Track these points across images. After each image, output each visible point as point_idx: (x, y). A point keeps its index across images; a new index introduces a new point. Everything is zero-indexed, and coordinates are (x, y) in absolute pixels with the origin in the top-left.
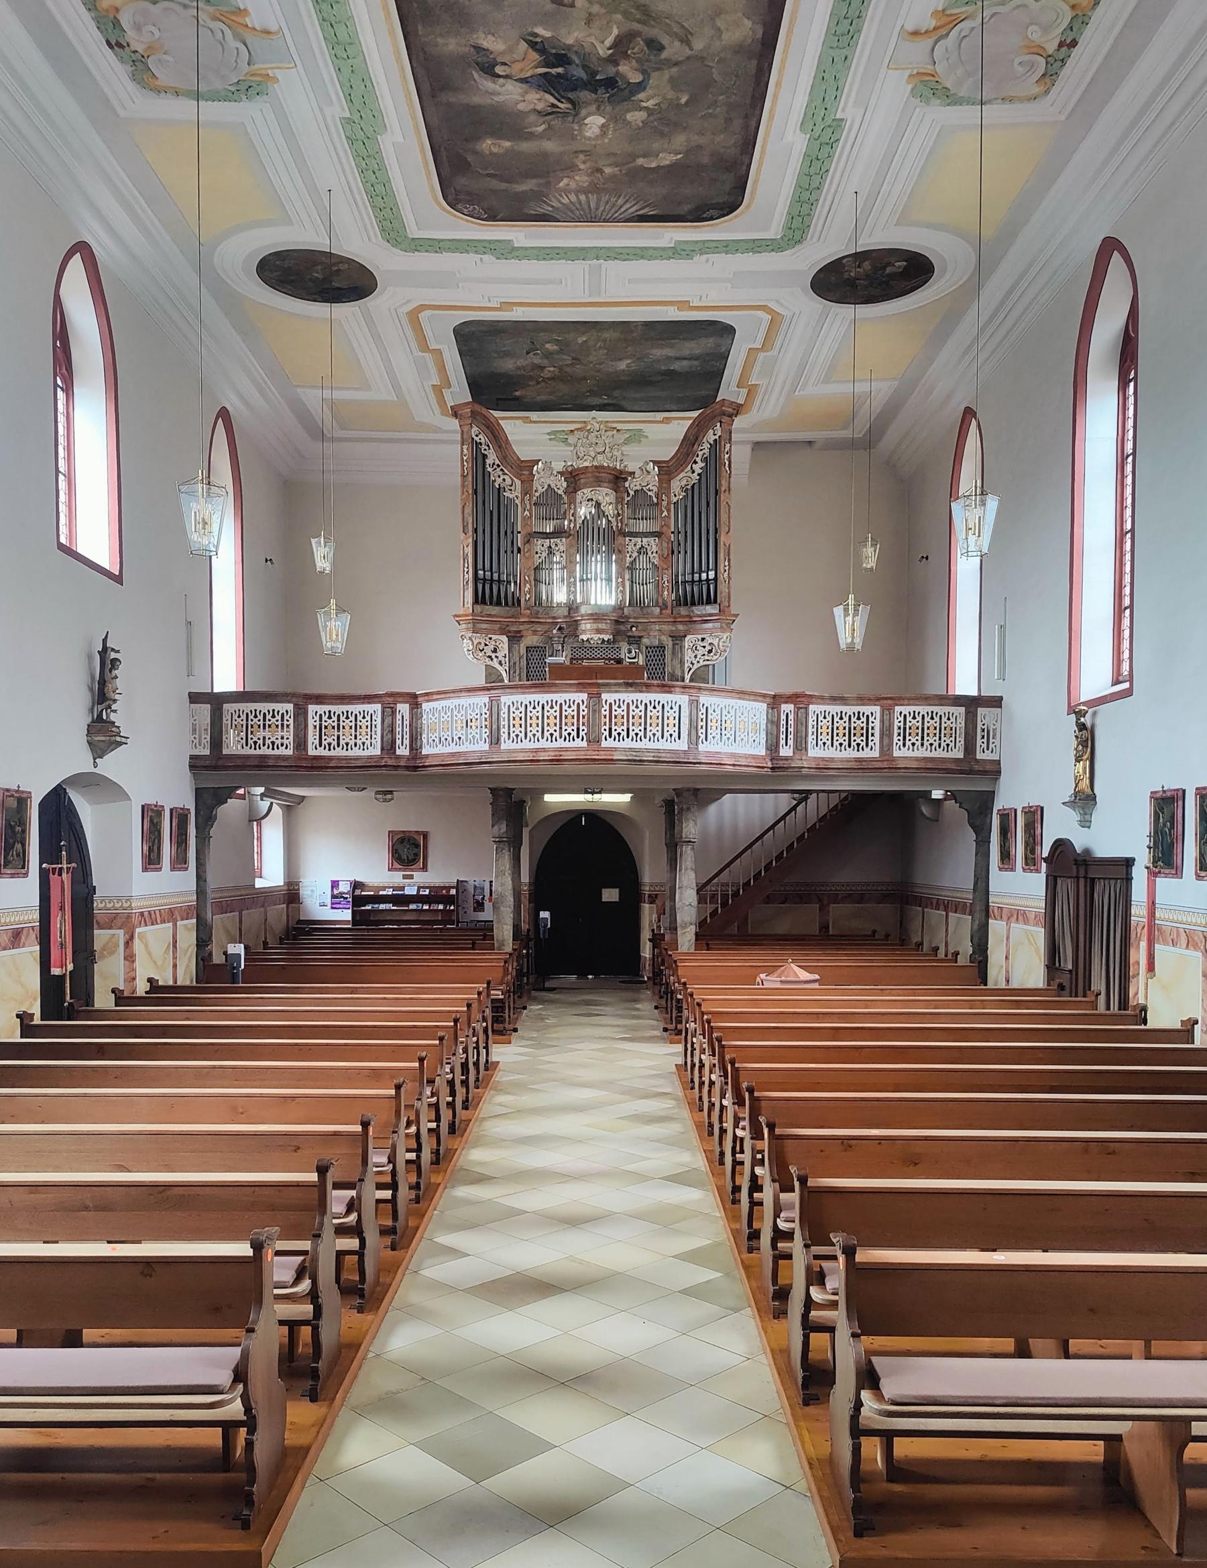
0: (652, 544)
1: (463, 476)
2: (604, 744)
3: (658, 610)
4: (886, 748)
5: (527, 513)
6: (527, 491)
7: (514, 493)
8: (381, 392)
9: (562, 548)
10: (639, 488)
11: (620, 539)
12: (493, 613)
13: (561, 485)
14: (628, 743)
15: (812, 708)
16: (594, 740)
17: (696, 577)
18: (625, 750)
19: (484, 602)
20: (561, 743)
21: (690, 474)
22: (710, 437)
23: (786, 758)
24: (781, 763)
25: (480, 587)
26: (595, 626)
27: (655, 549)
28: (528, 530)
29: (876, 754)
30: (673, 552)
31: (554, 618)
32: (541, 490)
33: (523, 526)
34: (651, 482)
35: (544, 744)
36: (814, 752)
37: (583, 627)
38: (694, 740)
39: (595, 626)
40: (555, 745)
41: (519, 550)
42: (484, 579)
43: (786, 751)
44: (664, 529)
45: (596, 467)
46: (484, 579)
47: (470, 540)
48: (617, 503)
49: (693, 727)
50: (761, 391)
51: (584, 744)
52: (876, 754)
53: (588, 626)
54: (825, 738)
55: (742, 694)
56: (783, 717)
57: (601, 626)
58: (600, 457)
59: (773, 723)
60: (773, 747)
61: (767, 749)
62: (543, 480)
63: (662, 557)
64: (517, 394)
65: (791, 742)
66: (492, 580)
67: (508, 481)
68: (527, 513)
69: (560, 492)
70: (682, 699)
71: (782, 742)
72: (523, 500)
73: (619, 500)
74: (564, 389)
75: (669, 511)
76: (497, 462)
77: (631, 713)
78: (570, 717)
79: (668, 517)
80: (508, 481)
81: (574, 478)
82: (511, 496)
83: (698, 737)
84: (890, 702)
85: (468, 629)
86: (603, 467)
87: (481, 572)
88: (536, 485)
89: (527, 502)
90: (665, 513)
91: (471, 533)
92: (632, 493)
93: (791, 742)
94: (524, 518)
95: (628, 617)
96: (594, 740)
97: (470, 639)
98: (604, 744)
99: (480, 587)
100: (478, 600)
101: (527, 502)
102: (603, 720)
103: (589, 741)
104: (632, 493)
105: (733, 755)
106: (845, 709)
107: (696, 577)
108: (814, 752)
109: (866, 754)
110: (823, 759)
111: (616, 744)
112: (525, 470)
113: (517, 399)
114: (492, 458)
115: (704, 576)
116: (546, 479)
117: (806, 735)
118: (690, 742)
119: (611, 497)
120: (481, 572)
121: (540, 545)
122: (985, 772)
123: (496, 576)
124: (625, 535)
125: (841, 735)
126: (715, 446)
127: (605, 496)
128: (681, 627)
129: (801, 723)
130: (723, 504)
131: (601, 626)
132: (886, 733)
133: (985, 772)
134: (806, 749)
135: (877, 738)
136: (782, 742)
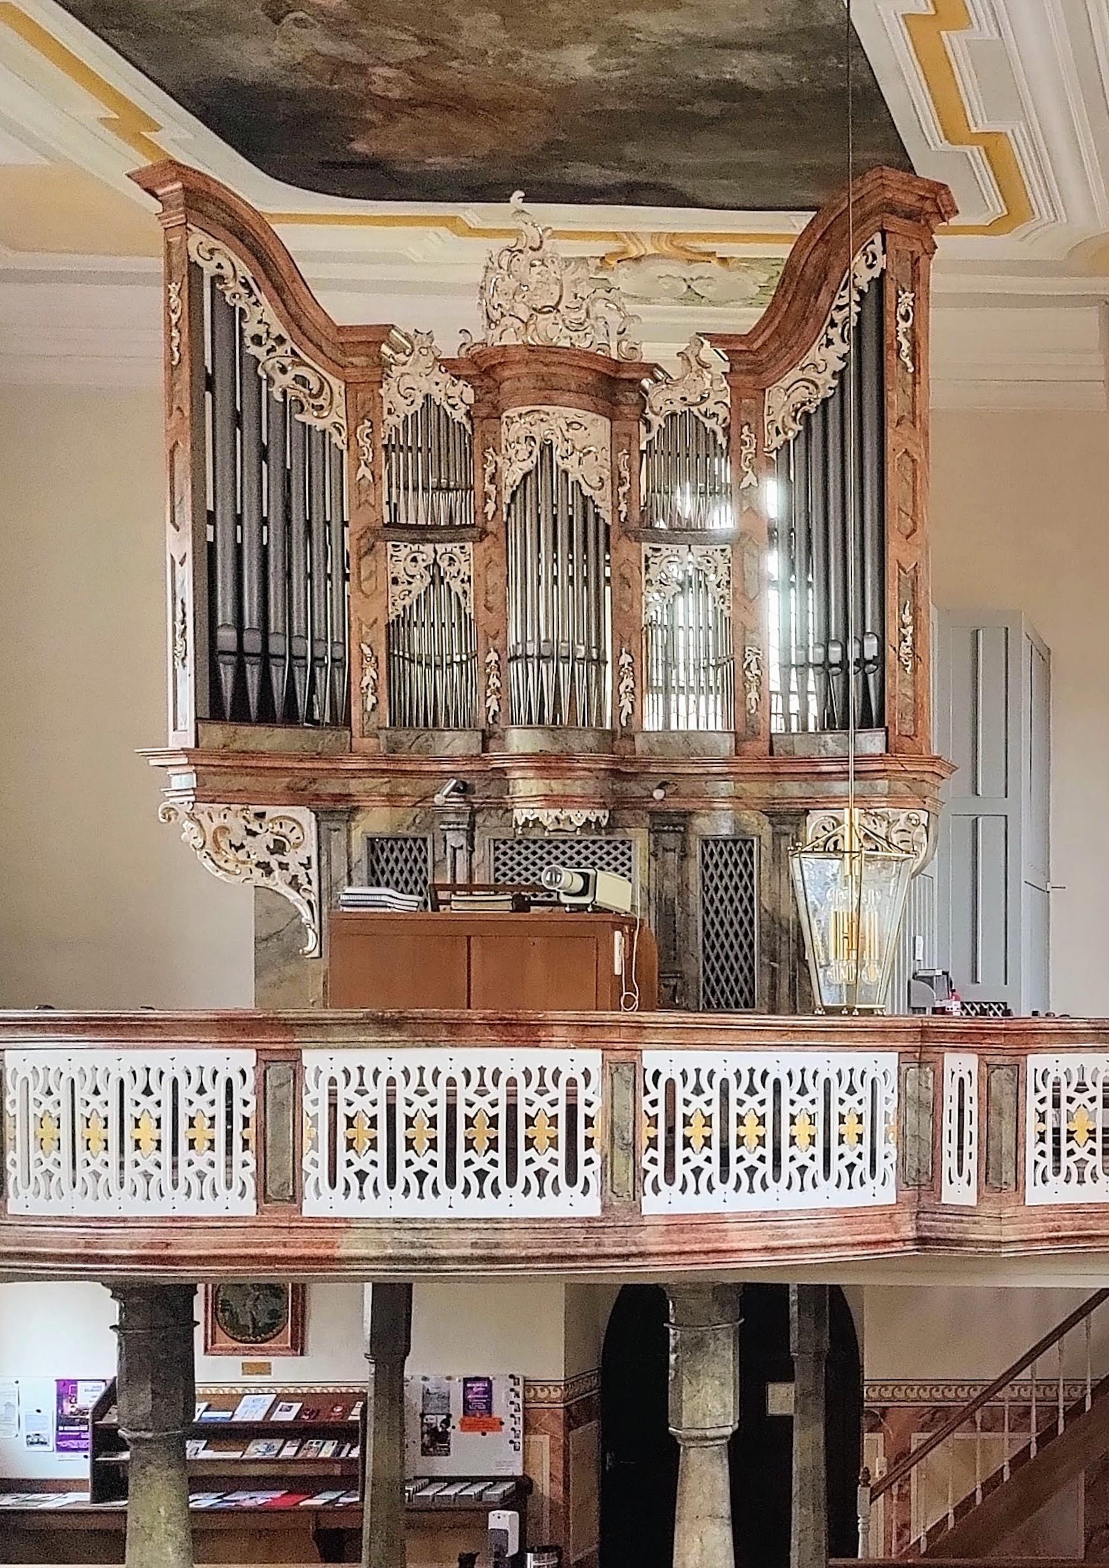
5: (364, 471)
6: (365, 410)
11: (625, 549)
12: (266, 746)
25: (227, 675)
32: (404, 409)
48: (615, 448)
62: (412, 384)
68: (364, 471)
69: (459, 415)
73: (620, 441)
82: (319, 425)
87: (227, 638)
89: (365, 443)
99: (227, 675)
104: (657, 421)
112: (366, 352)
114: (263, 316)
121: (405, 561)
123: (277, 645)
128: (794, 789)
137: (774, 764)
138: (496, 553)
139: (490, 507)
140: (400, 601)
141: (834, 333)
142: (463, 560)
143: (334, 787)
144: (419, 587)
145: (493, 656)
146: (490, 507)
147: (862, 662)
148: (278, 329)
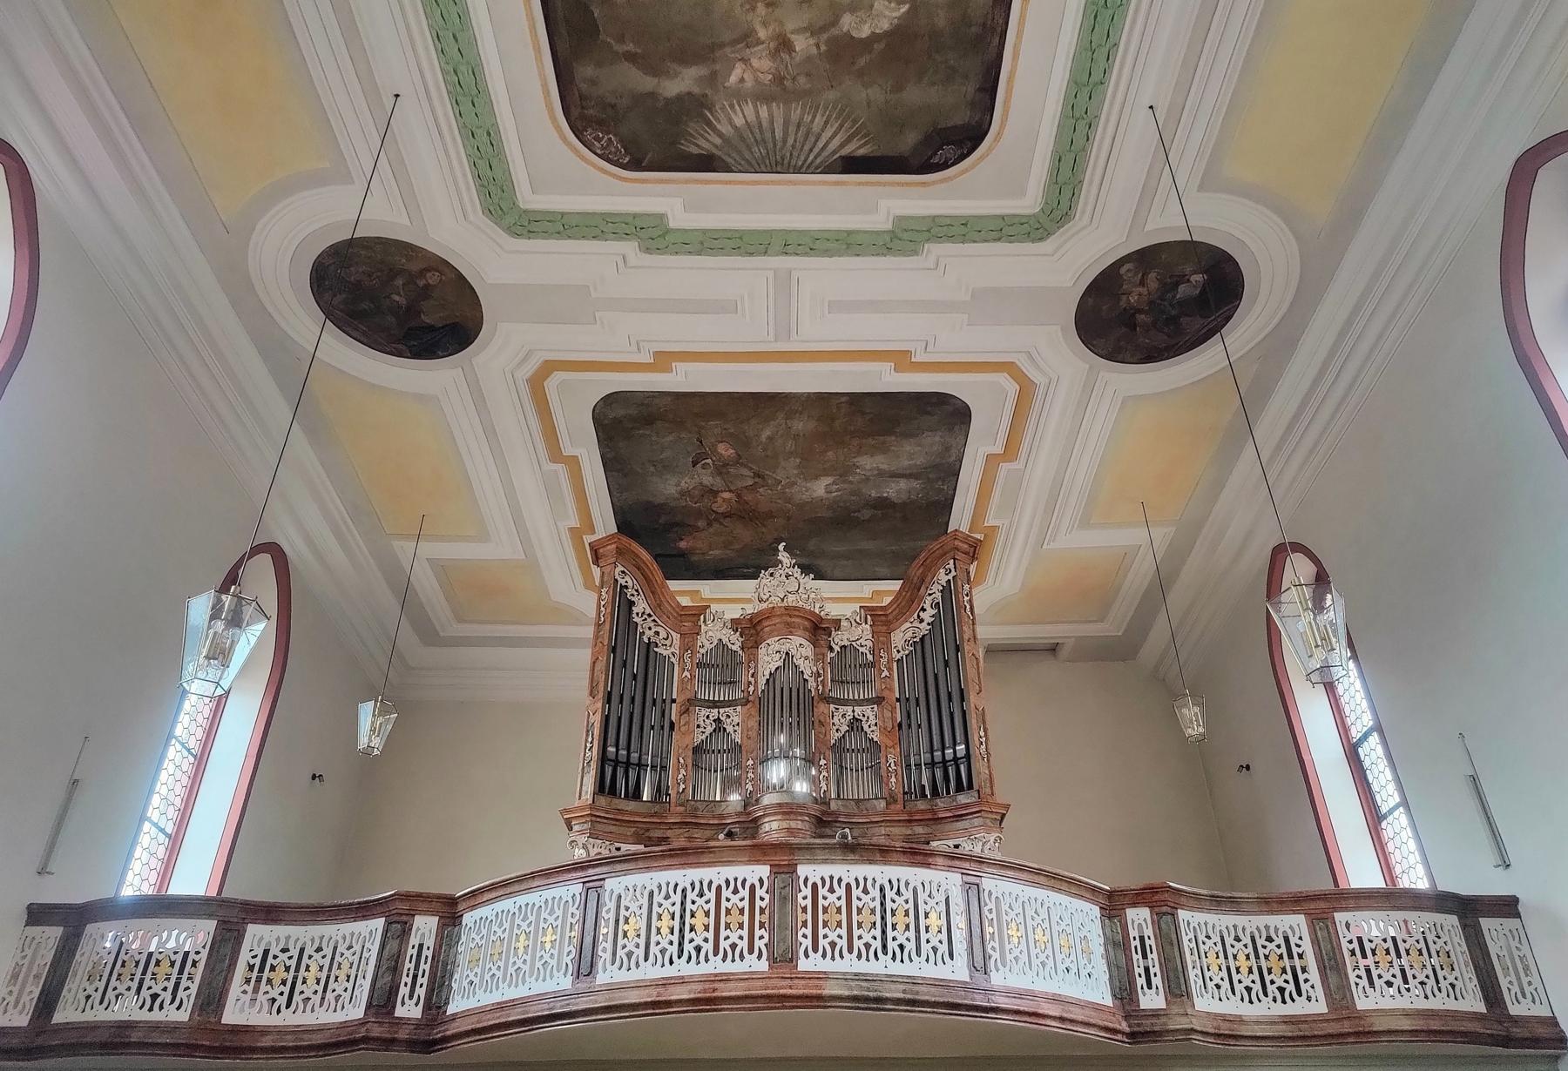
0: (868, 713)
1: (599, 625)
2: (804, 965)
3: (883, 804)
4: (1339, 993)
5: (686, 673)
7: (670, 647)
8: (501, 548)
9: (736, 720)
10: (846, 643)
11: (821, 708)
13: (735, 642)
14: (849, 964)
15: (1182, 915)
16: (783, 958)
17: (938, 754)
18: (845, 978)
19: (613, 792)
20: (716, 966)
21: (916, 624)
22: (943, 577)
23: (1155, 1014)
24: (1147, 1025)
26: (785, 825)
27: (872, 721)
28: (689, 695)
29: (1320, 1007)
30: (900, 725)
31: (722, 817)
32: (708, 646)
33: (682, 690)
34: (859, 635)
35: (683, 968)
36: (1206, 1003)
37: (766, 827)
38: (980, 965)
39: (785, 825)
40: (705, 969)
41: (672, 725)
42: (616, 762)
43: (1152, 1000)
44: (886, 694)
45: (786, 608)
46: (616, 762)
47: (600, 705)
49: (977, 939)
50: (1000, 539)
51: (763, 965)
52: (1320, 1007)
53: (775, 825)
54: (1218, 976)
55: (1056, 881)
56: (1133, 933)
57: (793, 824)
58: (791, 598)
59: (1118, 945)
60: (1125, 992)
61: (1114, 996)
63: (883, 730)
64: (683, 544)
65: (1157, 981)
66: (628, 764)
67: (663, 634)
68: (686, 673)
70: (949, 881)
71: (1141, 981)
72: (681, 657)
73: (819, 657)
74: (744, 534)
75: (890, 669)
76: (648, 611)
77: (855, 903)
78: (735, 912)
79: (890, 677)
80: (663, 634)
81: (752, 629)
82: (665, 653)
83: (986, 957)
84: (1322, 905)
85: (581, 832)
86: (795, 609)
87: (612, 749)
88: (701, 640)
89: (688, 661)
90: (886, 673)
91: (601, 695)
92: (837, 648)
93: (1157, 981)
94: (682, 681)
95: (835, 814)
96: (783, 958)
97: (585, 847)
98: (804, 965)
100: (604, 787)
101: (688, 661)
102: (801, 917)
103: (773, 960)
104: (837, 648)
105: (1055, 999)
106: (1241, 920)
107: (938, 754)
108: (1206, 1003)
109: (1299, 1007)
110: (1225, 1018)
111: (826, 965)
113: (682, 554)
114: (641, 605)
115: (949, 752)
116: (713, 634)
117: (1184, 968)
118: (973, 967)
119: (808, 650)
120: (612, 749)
121: (704, 718)
122: (1535, 1042)
123: (635, 756)
124: (828, 700)
125: (1244, 970)
126: (946, 590)
127: (800, 647)
129: (1169, 941)
130: (968, 656)
131: (793, 824)
132: (1331, 964)
133: (1535, 1042)
134: (1189, 995)
135: (1314, 975)
136: (1141, 981)
137: (910, 814)
138: (754, 712)
139: (751, 689)
140: (699, 738)
141: (927, 606)
142: (734, 719)
143: (657, 834)
144: (709, 730)
145: (750, 762)
146: (751, 689)
147: (956, 759)
148: (648, 611)
